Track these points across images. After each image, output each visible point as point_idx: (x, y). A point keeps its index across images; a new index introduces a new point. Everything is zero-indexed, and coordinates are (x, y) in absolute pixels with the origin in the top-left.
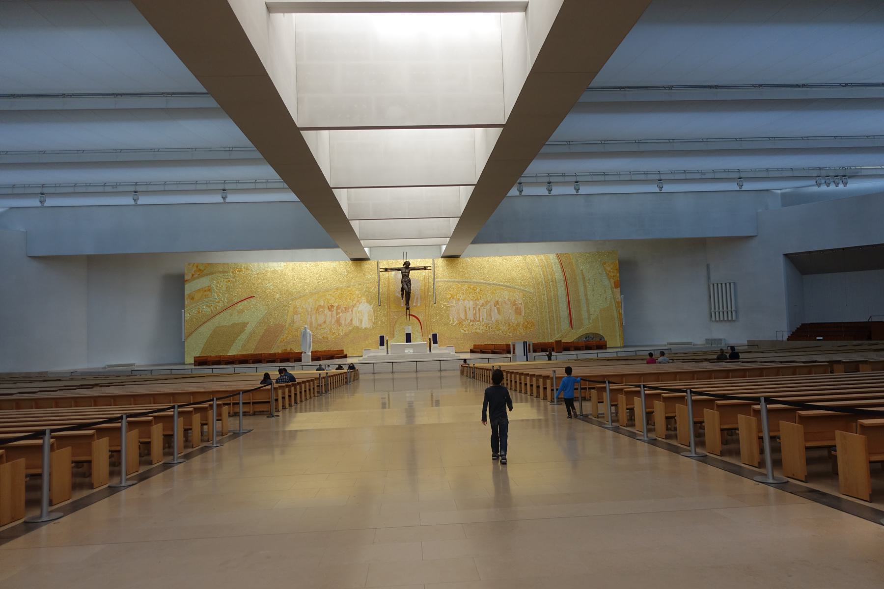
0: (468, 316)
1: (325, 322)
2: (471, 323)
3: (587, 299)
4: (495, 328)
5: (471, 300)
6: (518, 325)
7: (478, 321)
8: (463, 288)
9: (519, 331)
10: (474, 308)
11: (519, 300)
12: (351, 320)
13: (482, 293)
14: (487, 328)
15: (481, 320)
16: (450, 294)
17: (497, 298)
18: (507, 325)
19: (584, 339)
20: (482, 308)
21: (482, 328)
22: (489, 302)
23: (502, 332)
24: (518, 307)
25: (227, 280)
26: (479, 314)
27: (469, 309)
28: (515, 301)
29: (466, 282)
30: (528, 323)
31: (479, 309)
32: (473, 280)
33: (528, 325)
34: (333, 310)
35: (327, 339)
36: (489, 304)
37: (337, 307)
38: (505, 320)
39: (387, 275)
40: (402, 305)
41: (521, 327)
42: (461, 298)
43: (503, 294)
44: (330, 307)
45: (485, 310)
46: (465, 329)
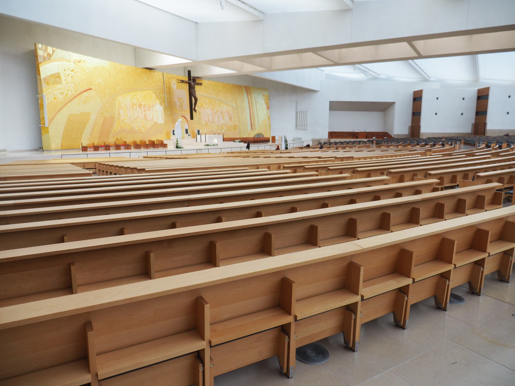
1: (138, 117)
2: (211, 124)
3: (257, 114)
5: (211, 109)
6: (231, 127)
12: (153, 117)
14: (218, 127)
15: (215, 123)
19: (257, 136)
20: (215, 114)
25: (71, 70)
27: (210, 115)
34: (141, 107)
35: (141, 131)
37: (144, 105)
39: (169, 85)
40: (178, 109)
44: (140, 105)
45: (217, 116)
46: (209, 128)
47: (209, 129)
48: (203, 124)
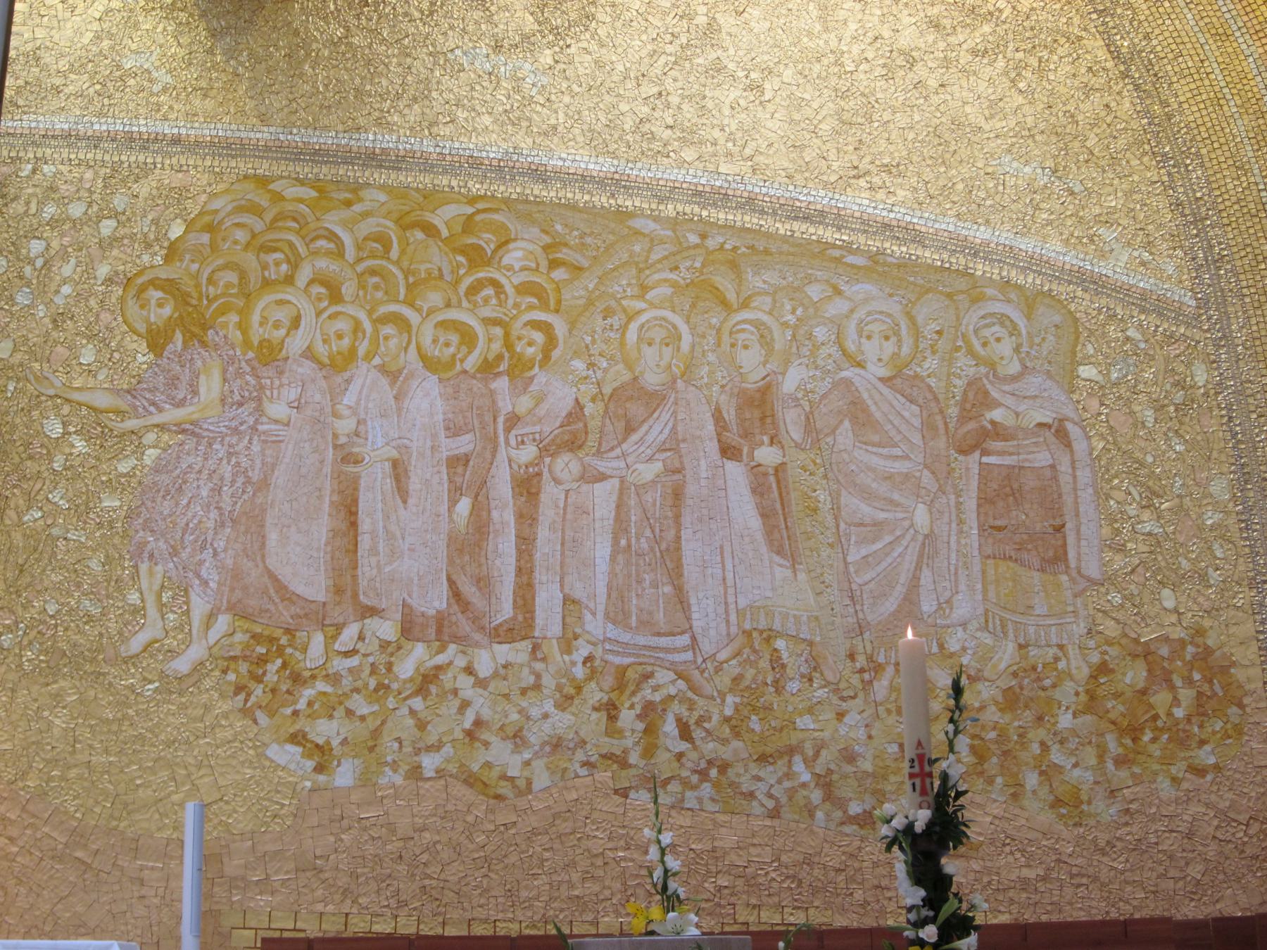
0: (366, 569)
4: (736, 726)
5: (430, 364)
7: (506, 634)
8: (332, 221)
9: (1048, 773)
10: (457, 462)
11: (1034, 383)
13: (575, 294)
16: (169, 286)
17: (751, 362)
18: (881, 687)
20: (566, 465)
21: (562, 722)
22: (654, 400)
23: (825, 783)
24: (1012, 474)
26: (525, 544)
27: (399, 470)
28: (977, 399)
29: (373, 159)
30: (1160, 675)
31: (527, 486)
32: (468, 145)
33: (1161, 699)
36: (656, 430)
38: (861, 629)
41: (1065, 721)
42: (297, 344)
43: (837, 307)
45: (602, 497)
46: (325, 730)
47: (323, 757)
48: (182, 665)
